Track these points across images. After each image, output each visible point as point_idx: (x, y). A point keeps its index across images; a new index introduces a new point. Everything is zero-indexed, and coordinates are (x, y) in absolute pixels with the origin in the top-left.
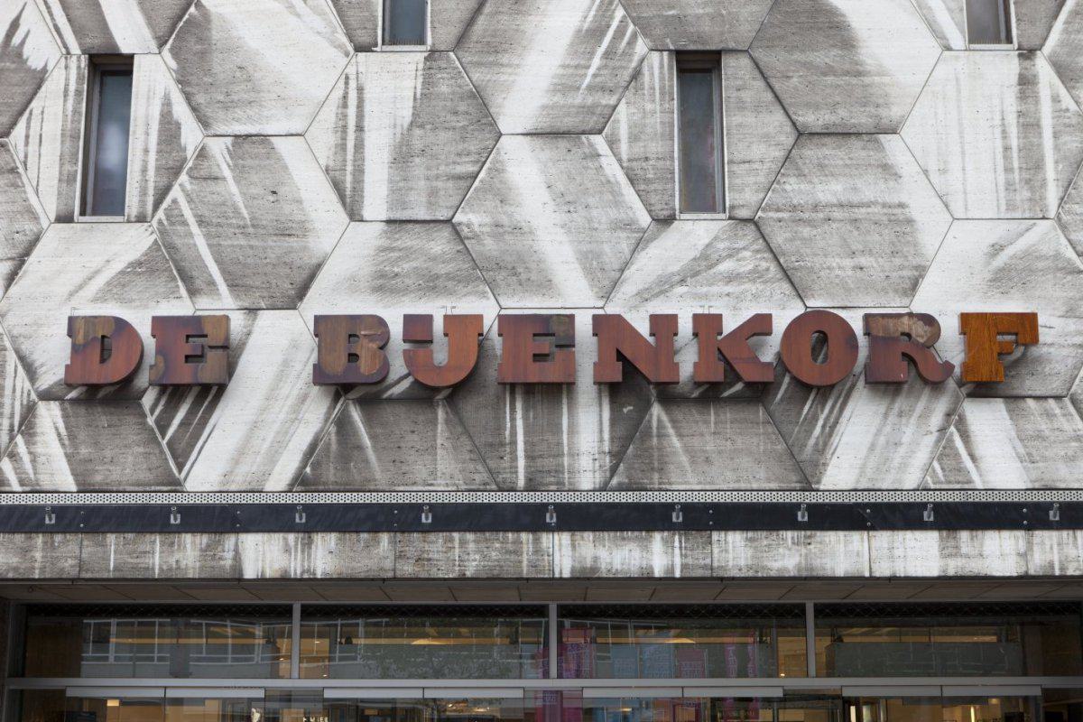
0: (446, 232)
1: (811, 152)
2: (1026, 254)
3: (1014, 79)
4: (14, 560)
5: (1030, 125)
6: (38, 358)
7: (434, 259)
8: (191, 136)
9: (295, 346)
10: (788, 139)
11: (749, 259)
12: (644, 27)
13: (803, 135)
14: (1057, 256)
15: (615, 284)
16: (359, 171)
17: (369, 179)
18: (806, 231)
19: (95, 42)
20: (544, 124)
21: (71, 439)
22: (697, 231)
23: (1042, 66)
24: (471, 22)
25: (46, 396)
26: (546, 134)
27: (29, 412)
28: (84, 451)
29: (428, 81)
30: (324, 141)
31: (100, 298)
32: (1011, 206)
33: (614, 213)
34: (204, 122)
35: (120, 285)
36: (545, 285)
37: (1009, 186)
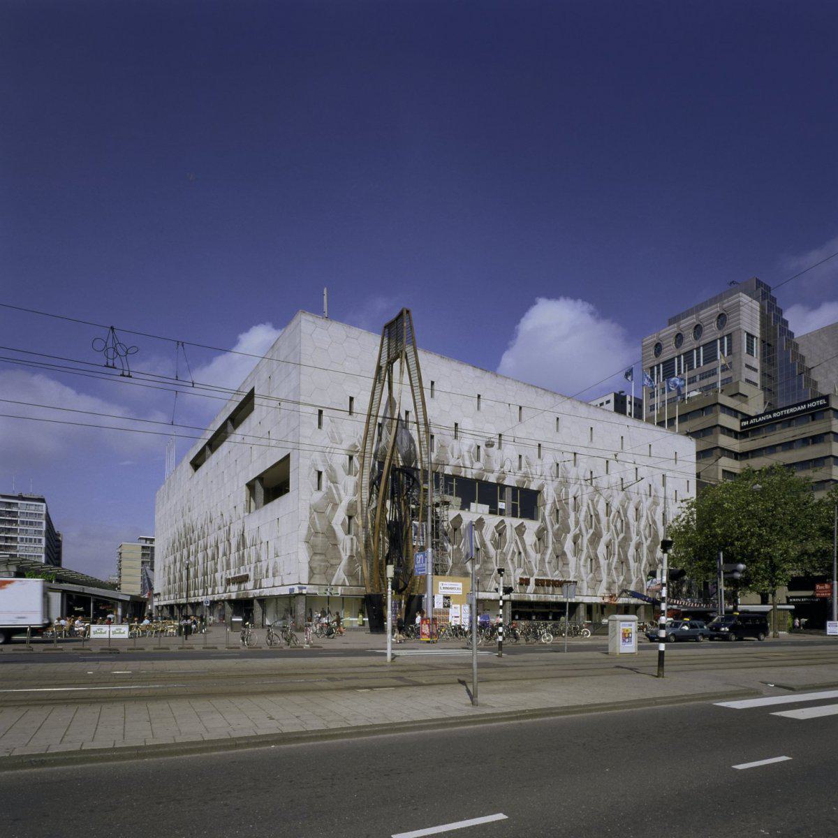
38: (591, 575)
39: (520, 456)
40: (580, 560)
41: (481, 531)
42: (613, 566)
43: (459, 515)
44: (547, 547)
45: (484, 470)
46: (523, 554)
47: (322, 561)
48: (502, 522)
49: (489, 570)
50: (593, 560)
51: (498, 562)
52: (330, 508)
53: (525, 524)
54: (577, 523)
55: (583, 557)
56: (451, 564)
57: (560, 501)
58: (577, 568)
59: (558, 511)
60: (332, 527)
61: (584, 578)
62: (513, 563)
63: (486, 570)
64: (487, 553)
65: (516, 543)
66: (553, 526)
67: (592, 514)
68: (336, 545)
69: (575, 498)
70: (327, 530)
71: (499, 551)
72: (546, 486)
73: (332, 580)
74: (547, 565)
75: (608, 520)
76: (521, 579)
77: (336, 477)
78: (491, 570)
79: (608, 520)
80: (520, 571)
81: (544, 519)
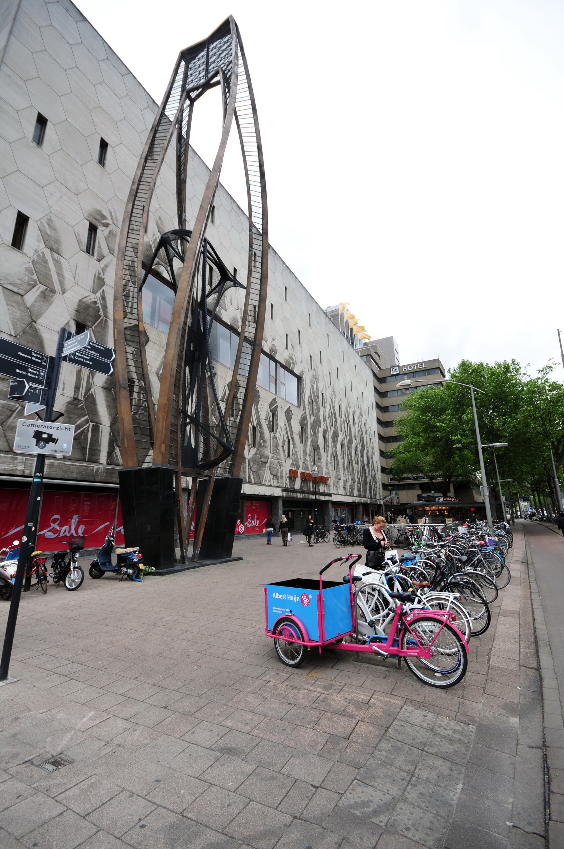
42: (346, 466)
57: (314, 393)
59: (313, 401)
60: (36, 330)
62: (284, 451)
63: (262, 456)
70: (24, 332)
71: (273, 434)
76: (290, 471)
77: (57, 242)
80: (289, 462)
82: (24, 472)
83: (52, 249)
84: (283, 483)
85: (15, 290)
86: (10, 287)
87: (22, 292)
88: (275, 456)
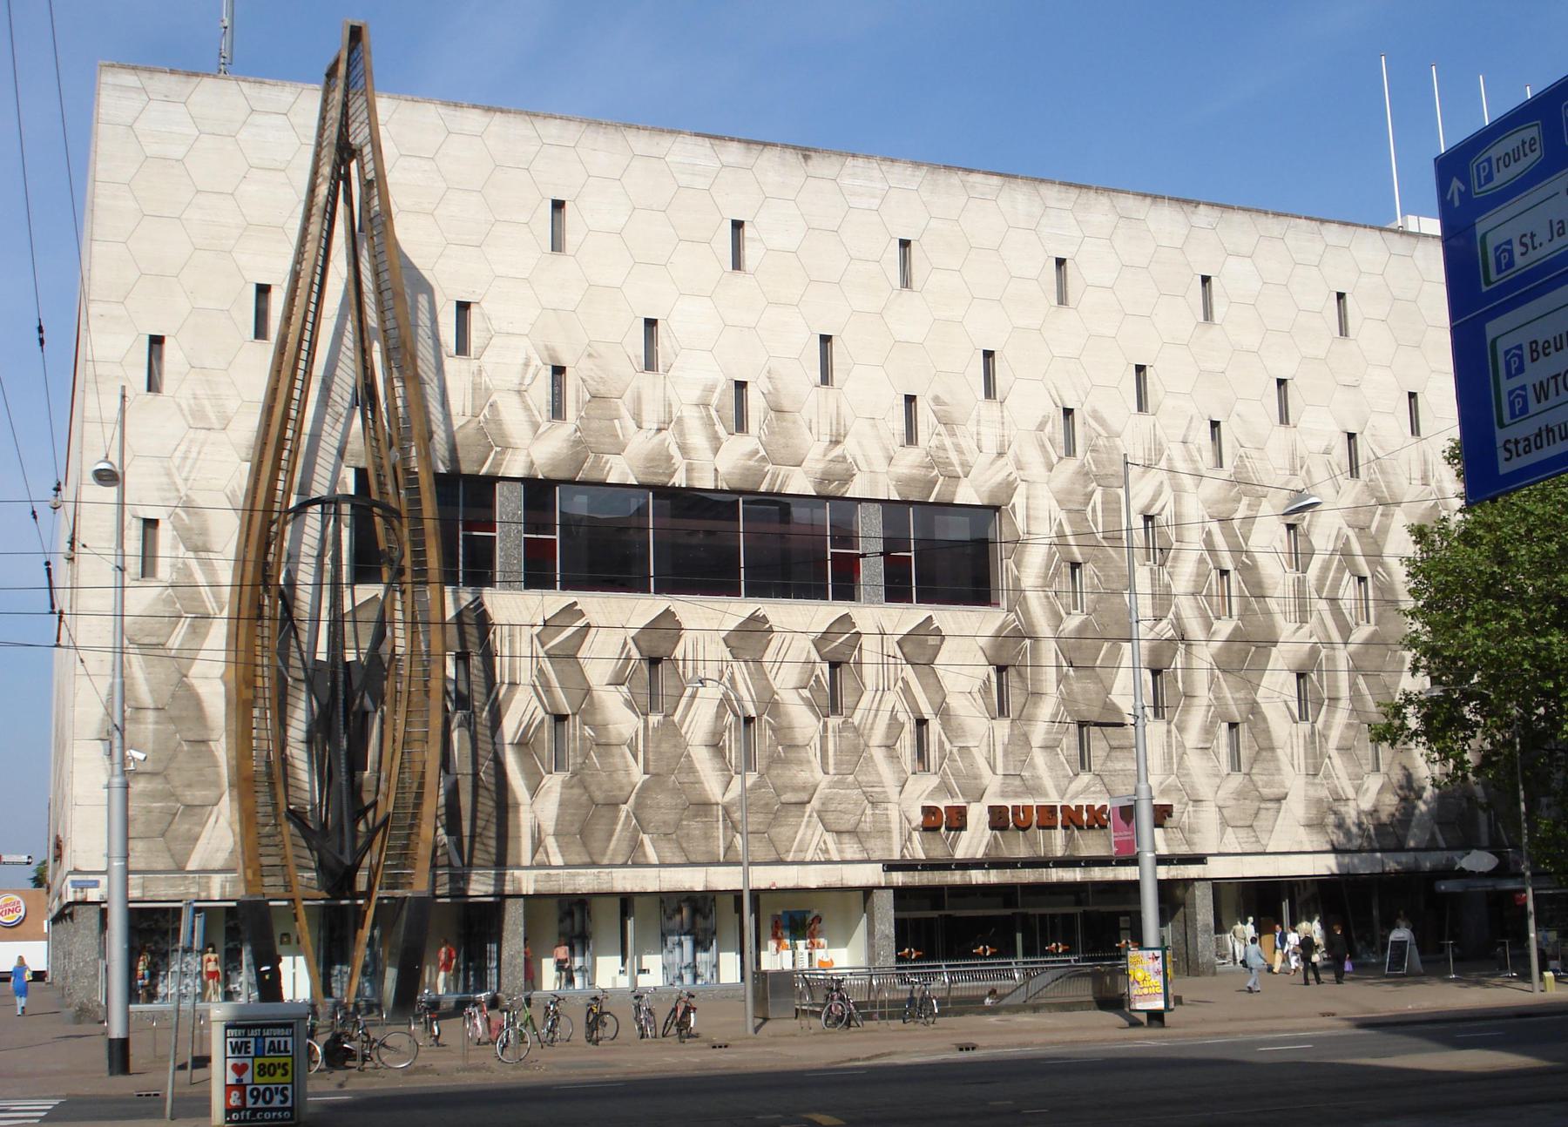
0: (1019, 778)
1: (1114, 754)
2: (1169, 785)
3: (1165, 731)
4: (910, 880)
5: (1170, 746)
6: (911, 817)
7: (1016, 786)
8: (947, 746)
9: (981, 814)
10: (1108, 749)
11: (1099, 787)
12: (1069, 714)
13: (1112, 748)
14: (1176, 786)
15: (1064, 794)
16: (995, 758)
17: (997, 761)
18: (1113, 778)
19: (918, 715)
20: (1043, 744)
21: (922, 842)
22: (1085, 778)
23: (1173, 727)
24: (1022, 711)
25: (915, 829)
26: (1044, 747)
27: (910, 834)
28: (926, 846)
29: (1012, 730)
30: (984, 749)
31: (927, 798)
32: (1165, 770)
33: (1063, 772)
34: (951, 742)
35: (931, 795)
36: (1046, 795)
37: (1165, 765)
38: (1237, 780)
39: (910, 400)
40: (1181, 729)
41: (758, 662)
43: (668, 614)
44: (1036, 695)
45: (763, 459)
46: (935, 726)
47: (153, 796)
48: (845, 619)
49: (795, 789)
50: (1243, 728)
51: (831, 761)
52: (183, 627)
53: (936, 623)
54: (1163, 599)
55: (1197, 718)
56: (638, 776)
57: (1083, 534)
58: (1175, 758)
61: (1204, 788)
64: (782, 732)
65: (907, 689)
66: (1057, 619)
67: (1228, 564)
68: (204, 742)
69: (1148, 518)
70: (173, 696)
71: (834, 721)
72: (1022, 489)
73: (188, 855)
74: (1040, 758)
75: (1301, 583)
76: (928, 811)
77: (204, 532)
78: (804, 788)
79: (1301, 583)
81: (1019, 598)
82: (198, 894)
83: (196, 550)
84: (890, 850)
85: (154, 640)
86: (146, 640)
87: (162, 640)
88: (851, 778)
